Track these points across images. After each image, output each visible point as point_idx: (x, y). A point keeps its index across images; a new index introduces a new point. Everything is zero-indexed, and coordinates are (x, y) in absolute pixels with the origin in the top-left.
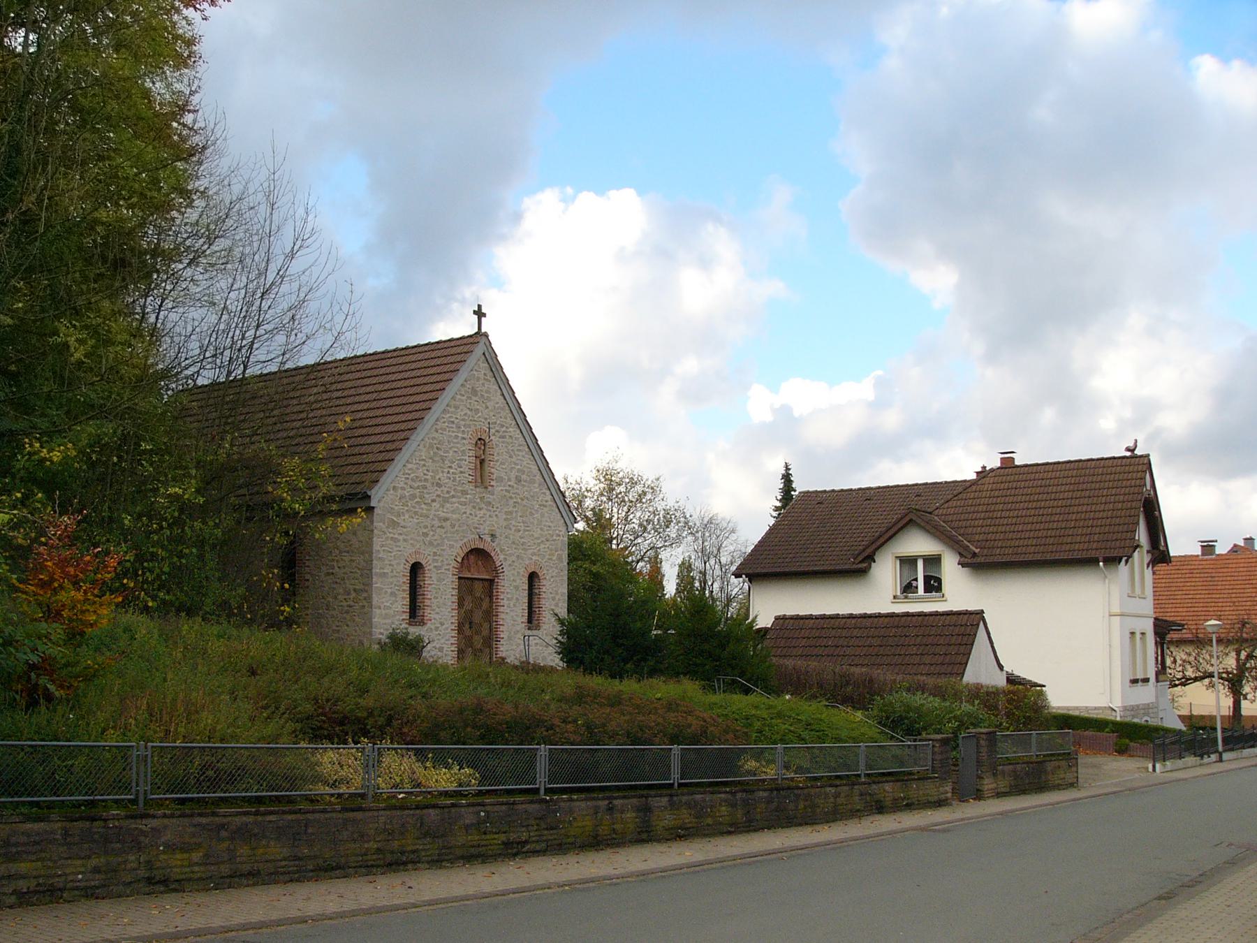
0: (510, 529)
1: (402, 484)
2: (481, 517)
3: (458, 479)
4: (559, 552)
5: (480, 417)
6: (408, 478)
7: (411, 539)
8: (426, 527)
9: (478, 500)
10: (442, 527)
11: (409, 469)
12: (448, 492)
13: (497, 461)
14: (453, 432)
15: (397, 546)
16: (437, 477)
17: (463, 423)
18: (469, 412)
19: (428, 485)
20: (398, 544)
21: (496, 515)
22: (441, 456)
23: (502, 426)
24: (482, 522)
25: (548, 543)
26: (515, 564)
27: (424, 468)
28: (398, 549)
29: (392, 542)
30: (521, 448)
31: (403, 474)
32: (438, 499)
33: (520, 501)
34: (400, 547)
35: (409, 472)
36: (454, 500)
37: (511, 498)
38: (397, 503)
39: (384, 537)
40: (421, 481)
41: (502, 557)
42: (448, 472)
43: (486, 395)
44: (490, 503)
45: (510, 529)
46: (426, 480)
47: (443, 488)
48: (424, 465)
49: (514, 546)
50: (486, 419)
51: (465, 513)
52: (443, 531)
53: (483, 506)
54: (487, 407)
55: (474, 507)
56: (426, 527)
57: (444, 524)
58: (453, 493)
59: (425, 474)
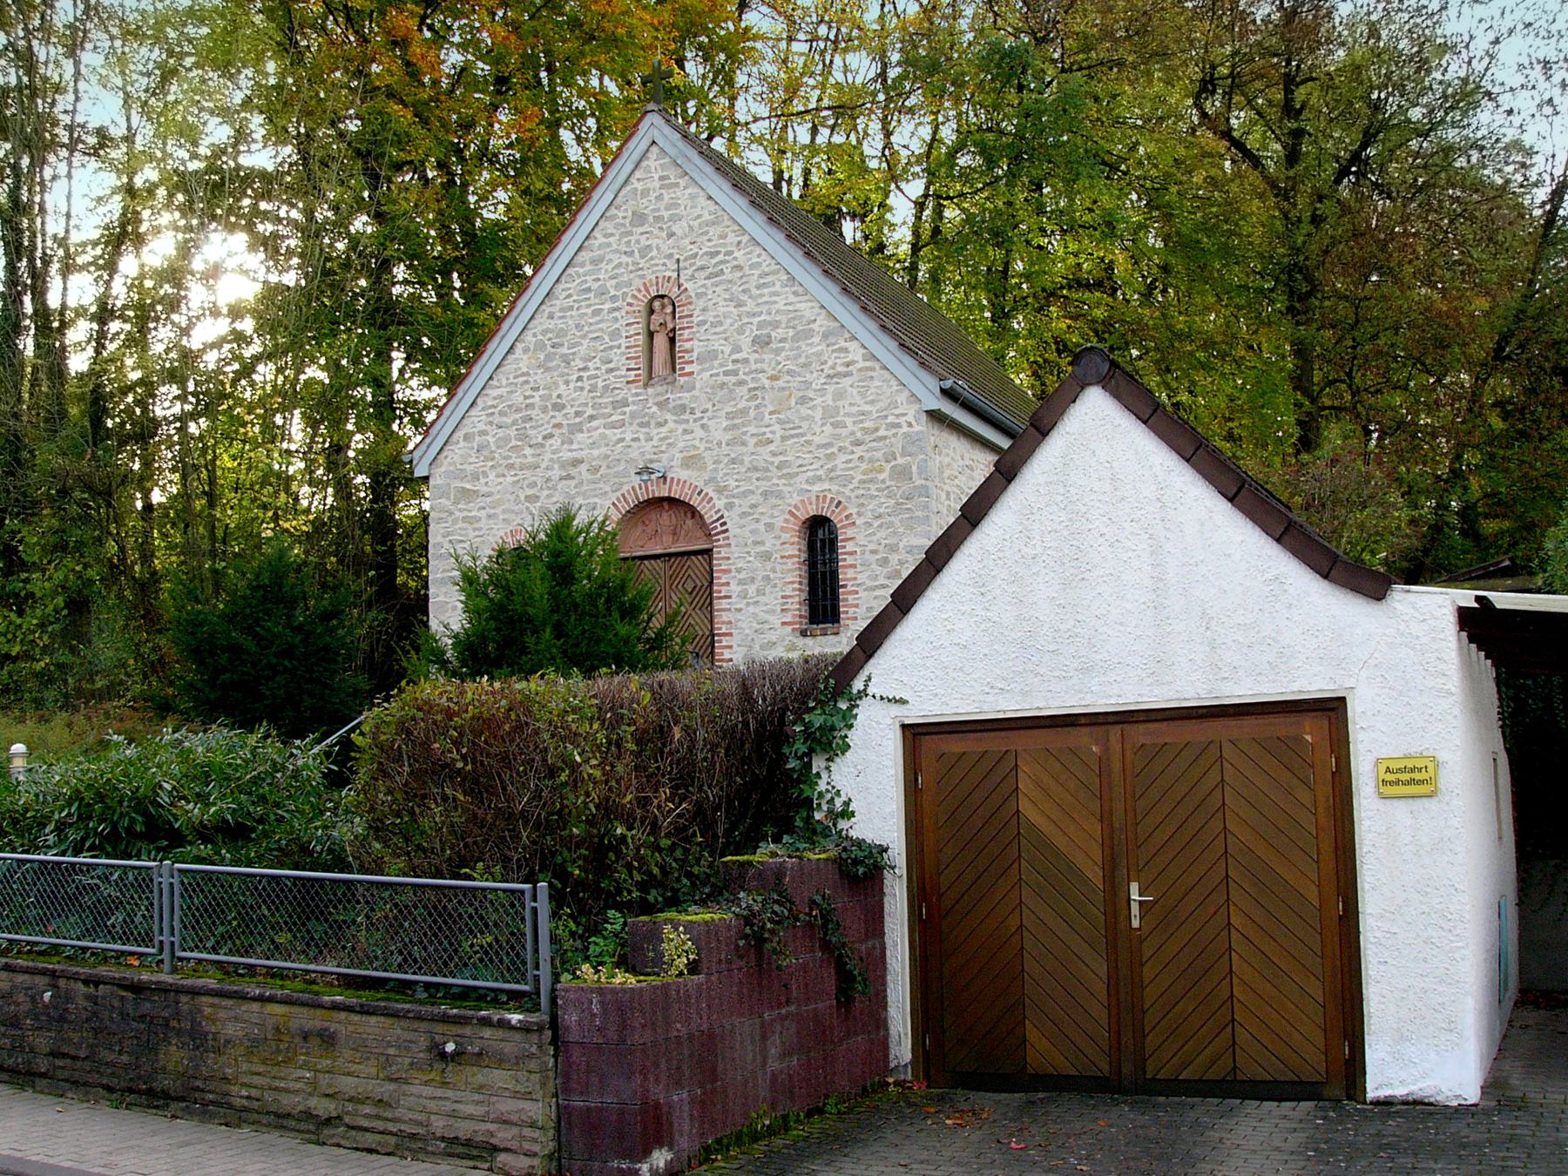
0: (744, 444)
1: (481, 427)
2: (661, 439)
3: (600, 384)
4: (900, 461)
5: (652, 258)
6: (493, 414)
7: (504, 511)
8: (533, 485)
9: (655, 409)
10: (569, 477)
11: (495, 398)
12: (577, 414)
13: (704, 322)
14: (589, 306)
15: (475, 530)
16: (555, 395)
17: (614, 282)
18: (625, 259)
19: (533, 413)
20: (476, 526)
21: (703, 426)
22: (562, 356)
23: (713, 254)
24: (663, 448)
25: (859, 451)
26: (760, 510)
27: (526, 387)
28: (477, 533)
29: (465, 525)
30: (769, 279)
31: (483, 409)
32: (557, 432)
33: (767, 383)
34: (479, 529)
35: (495, 403)
36: (595, 423)
37: (741, 383)
38: (471, 460)
39: (450, 519)
40: (518, 410)
41: (720, 503)
42: (580, 379)
43: (666, 214)
44: (683, 408)
45: (744, 444)
46: (530, 406)
47: (569, 410)
48: (527, 382)
49: (758, 475)
50: (670, 256)
51: (623, 440)
52: (572, 483)
53: (669, 417)
54: (671, 235)
55: (647, 425)
56: (533, 485)
57: (573, 472)
58: (590, 412)
59: (526, 398)
